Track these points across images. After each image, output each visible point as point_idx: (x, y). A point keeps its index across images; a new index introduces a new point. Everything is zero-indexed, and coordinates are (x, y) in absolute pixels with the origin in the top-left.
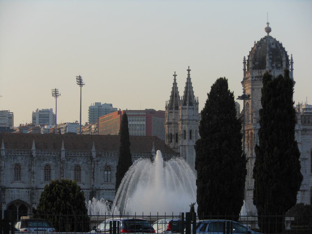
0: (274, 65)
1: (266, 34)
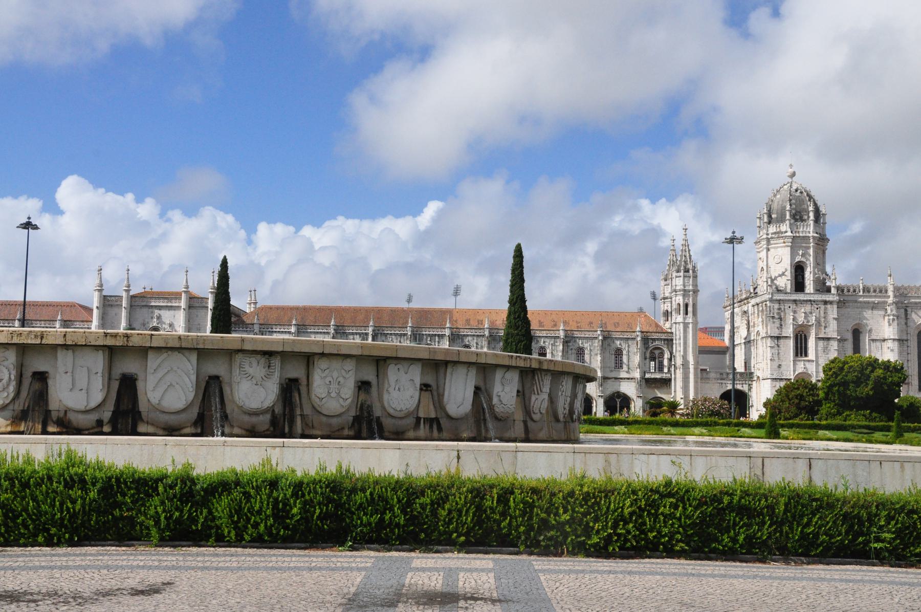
0: (798, 217)
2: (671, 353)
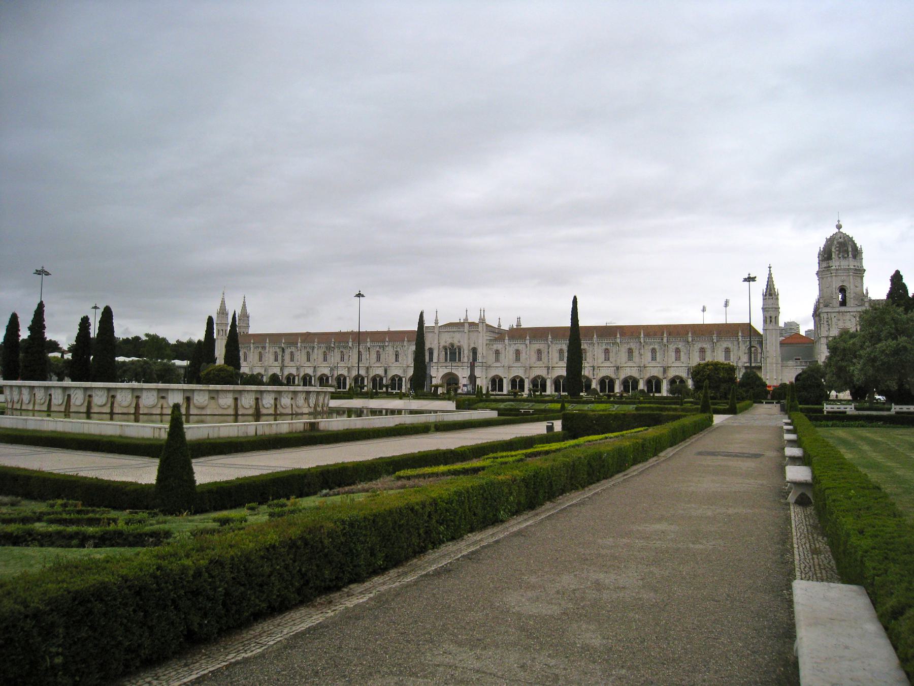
1: (837, 230)
2: (762, 350)
